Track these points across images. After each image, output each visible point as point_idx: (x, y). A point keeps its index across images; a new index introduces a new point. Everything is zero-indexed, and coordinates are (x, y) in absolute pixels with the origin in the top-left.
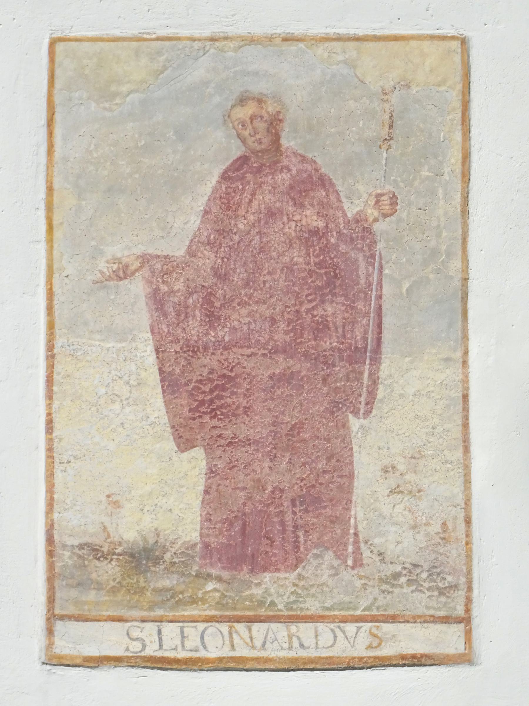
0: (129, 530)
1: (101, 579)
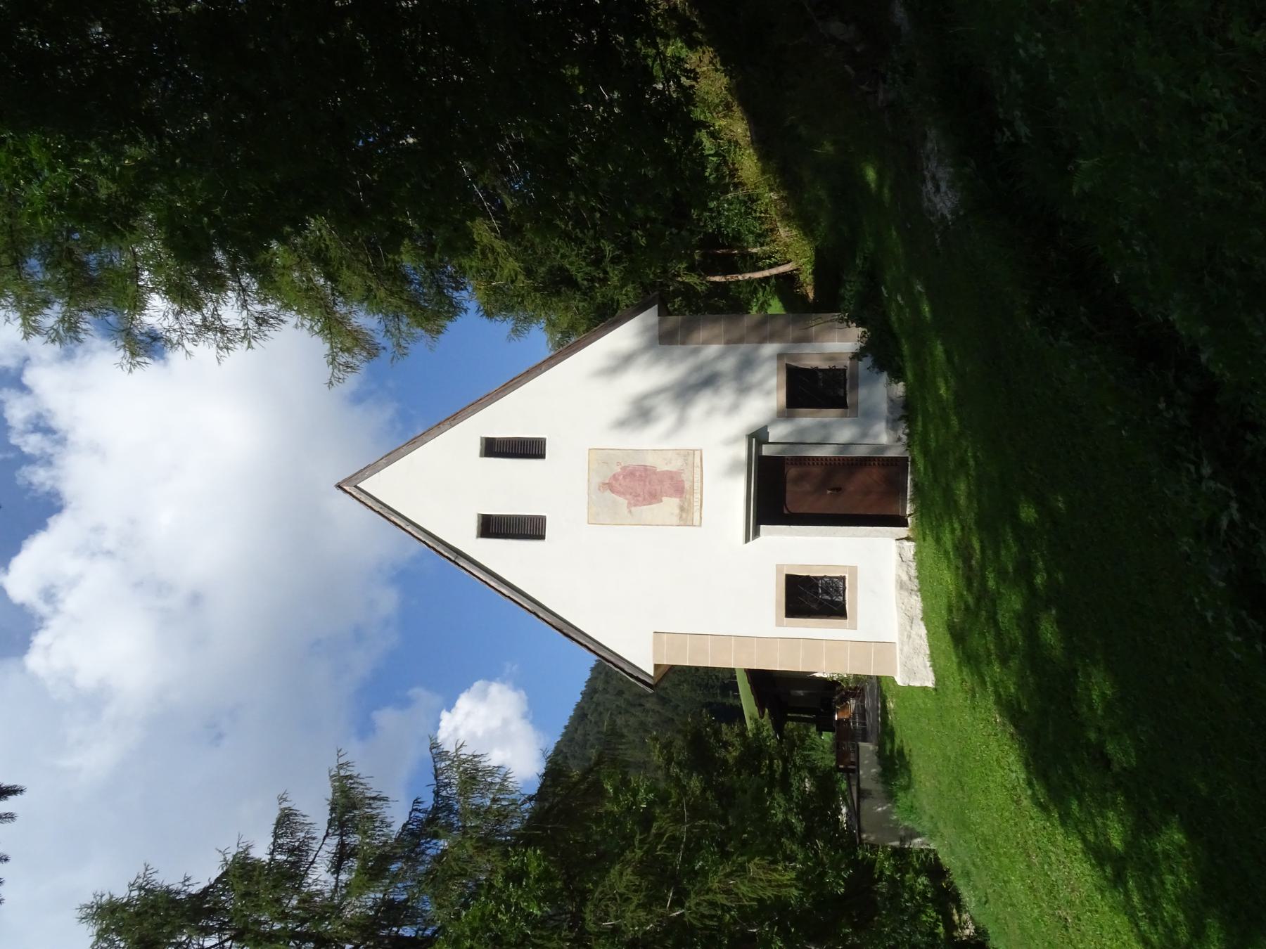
0: (677, 511)
1: (686, 516)
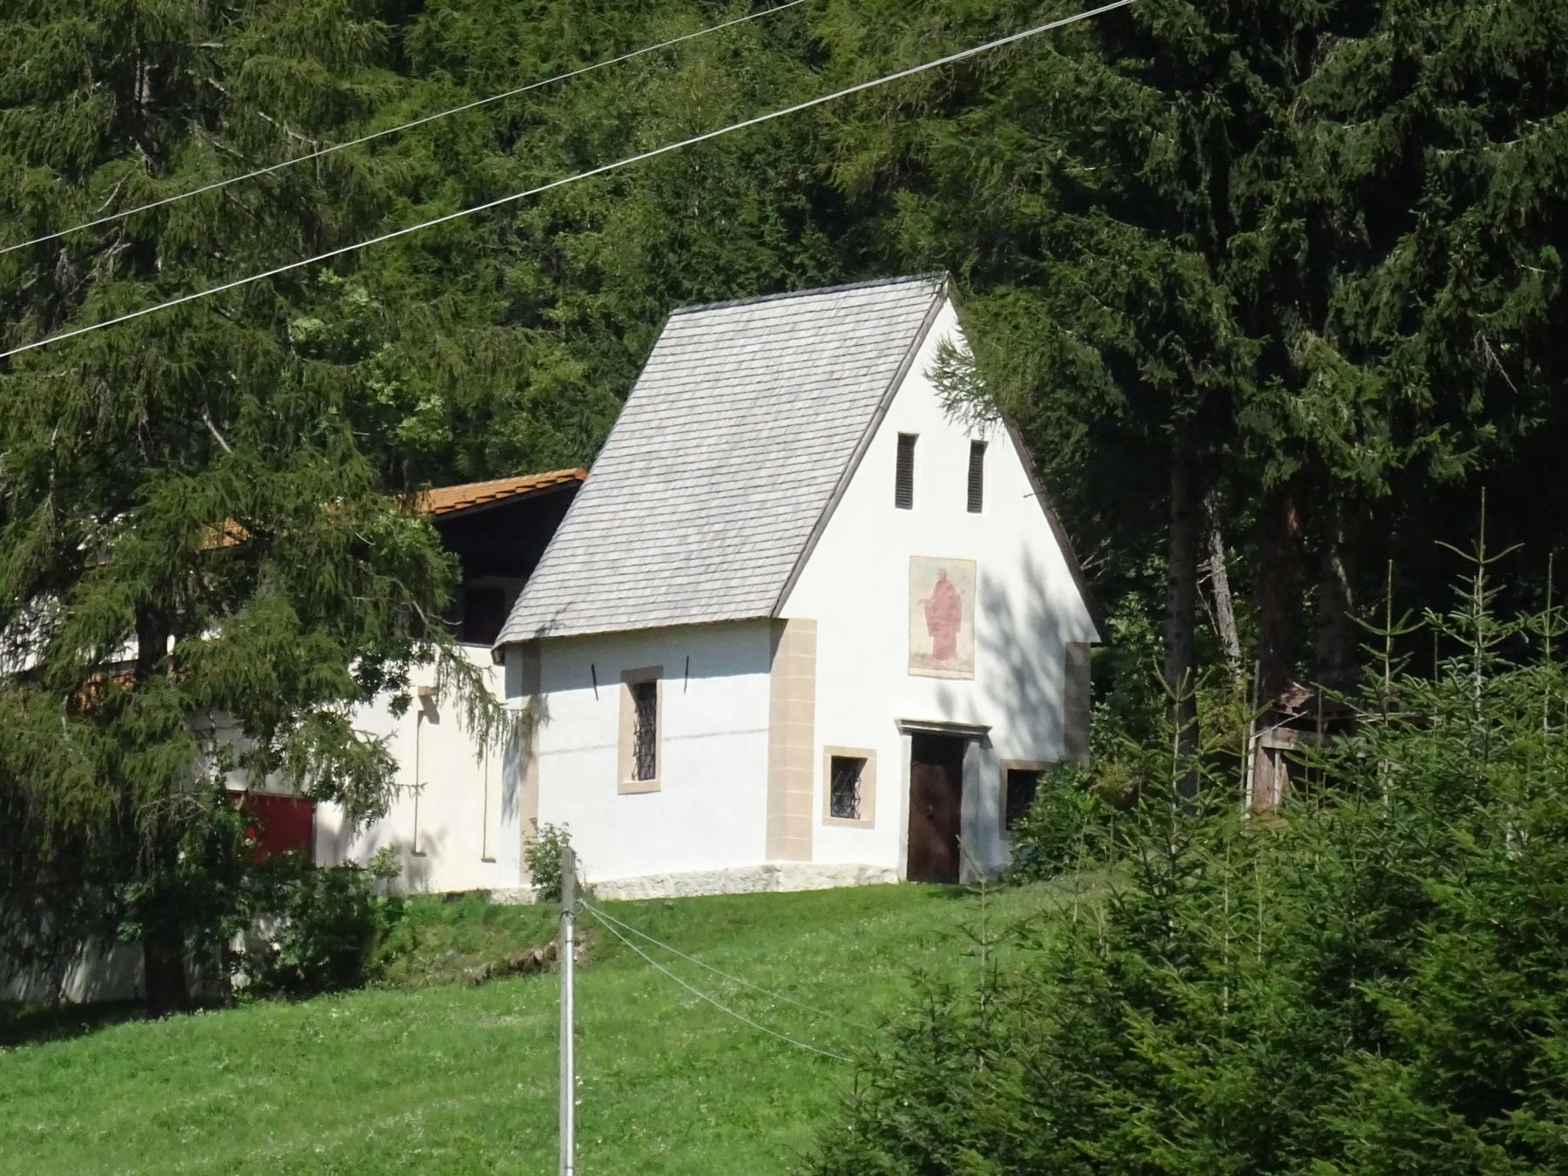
0: (922, 651)
1: (918, 659)
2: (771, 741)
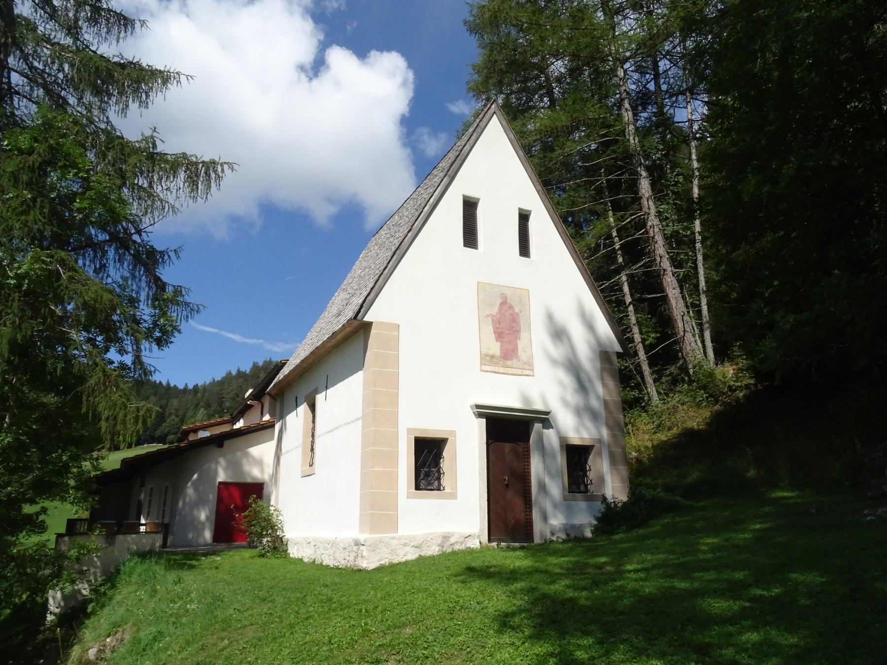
0: (491, 353)
1: (487, 359)
2: (363, 426)
